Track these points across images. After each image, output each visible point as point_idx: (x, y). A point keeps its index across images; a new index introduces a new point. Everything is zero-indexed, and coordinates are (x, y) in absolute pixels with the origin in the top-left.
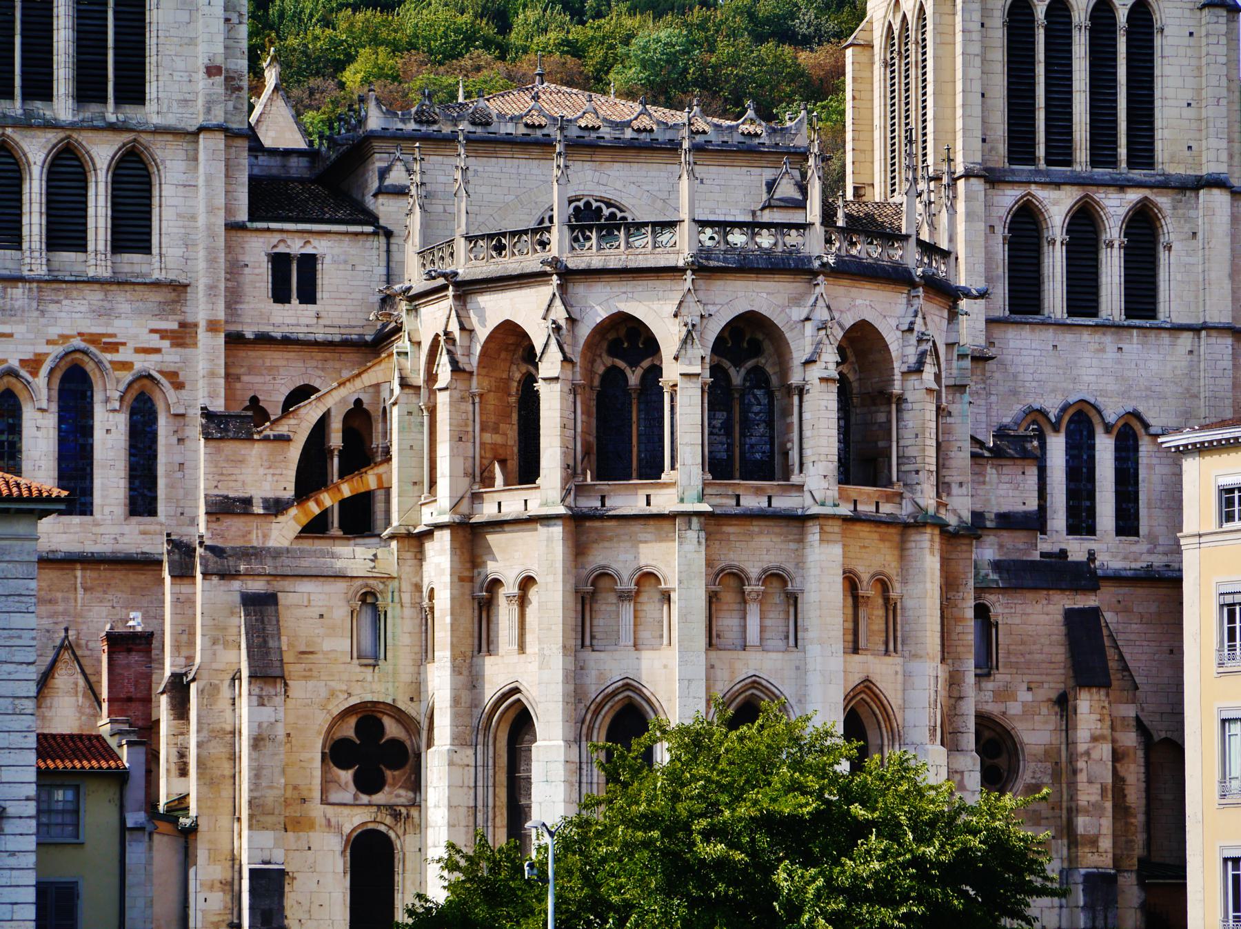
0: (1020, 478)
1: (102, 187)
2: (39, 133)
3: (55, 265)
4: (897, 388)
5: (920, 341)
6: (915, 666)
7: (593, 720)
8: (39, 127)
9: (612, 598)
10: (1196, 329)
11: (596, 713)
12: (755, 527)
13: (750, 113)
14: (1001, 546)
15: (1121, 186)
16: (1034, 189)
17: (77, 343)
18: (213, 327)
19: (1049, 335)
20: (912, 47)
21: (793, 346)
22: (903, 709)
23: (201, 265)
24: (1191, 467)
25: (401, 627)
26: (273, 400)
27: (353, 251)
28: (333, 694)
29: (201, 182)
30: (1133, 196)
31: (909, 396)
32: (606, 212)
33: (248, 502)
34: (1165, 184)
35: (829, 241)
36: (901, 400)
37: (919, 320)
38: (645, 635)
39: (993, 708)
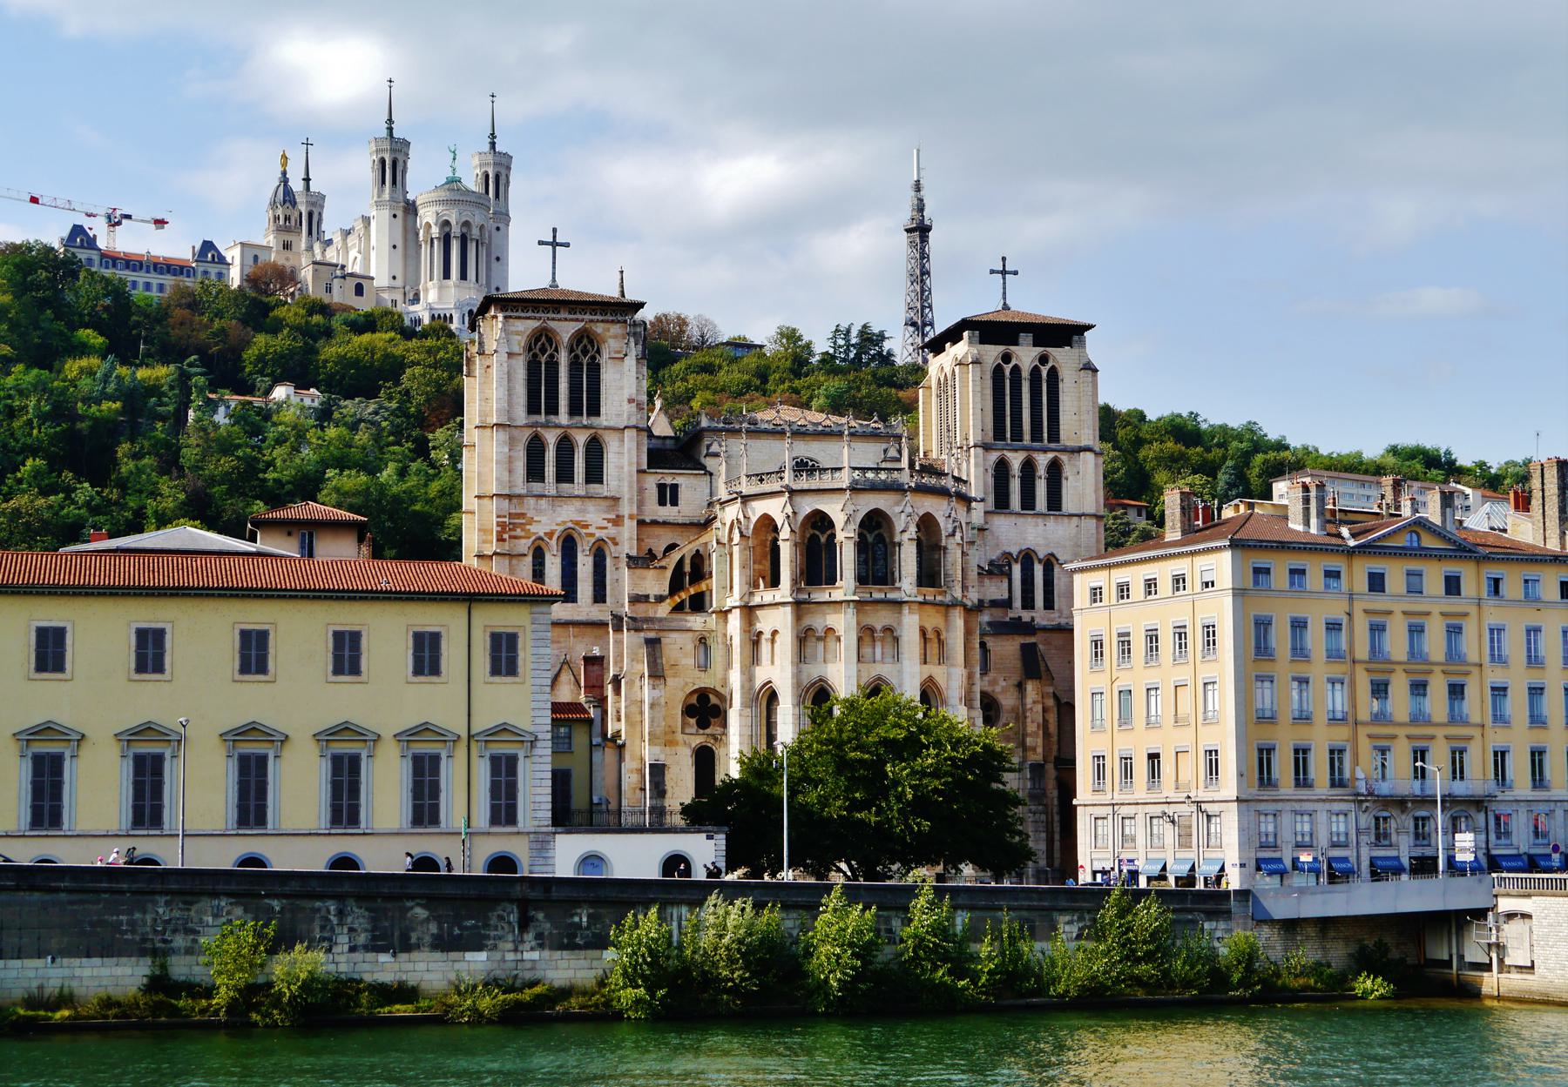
0: (999, 584)
1: (581, 454)
2: (552, 430)
3: (560, 490)
4: (943, 544)
5: (954, 521)
6: (953, 670)
7: (805, 696)
8: (552, 427)
9: (814, 639)
10: (1079, 516)
11: (807, 692)
12: (879, 607)
13: (876, 418)
14: (991, 615)
15: (1045, 451)
16: (1005, 452)
17: (570, 525)
18: (631, 517)
19: (1013, 519)
20: (949, 388)
21: (896, 524)
22: (947, 689)
23: (626, 489)
24: (1077, 578)
25: (717, 653)
26: (659, 551)
27: (695, 482)
28: (686, 684)
29: (626, 451)
30: (1051, 455)
31: (949, 547)
32: (810, 464)
33: (647, 597)
34: (1065, 450)
35: (912, 476)
36: (945, 548)
37: (953, 512)
38: (829, 656)
39: (988, 689)
